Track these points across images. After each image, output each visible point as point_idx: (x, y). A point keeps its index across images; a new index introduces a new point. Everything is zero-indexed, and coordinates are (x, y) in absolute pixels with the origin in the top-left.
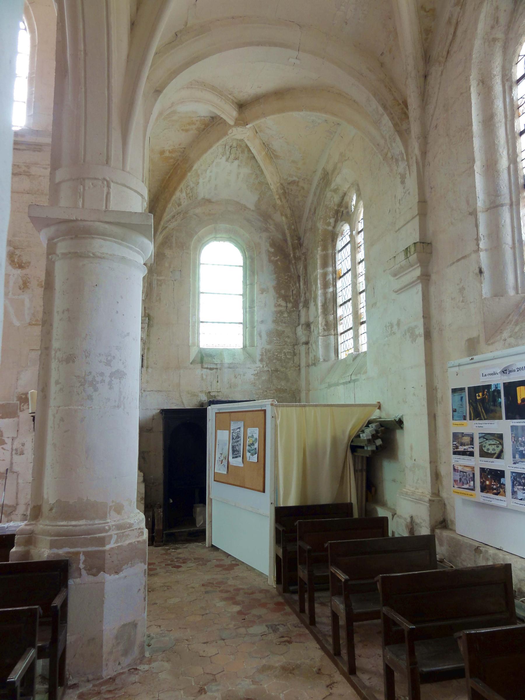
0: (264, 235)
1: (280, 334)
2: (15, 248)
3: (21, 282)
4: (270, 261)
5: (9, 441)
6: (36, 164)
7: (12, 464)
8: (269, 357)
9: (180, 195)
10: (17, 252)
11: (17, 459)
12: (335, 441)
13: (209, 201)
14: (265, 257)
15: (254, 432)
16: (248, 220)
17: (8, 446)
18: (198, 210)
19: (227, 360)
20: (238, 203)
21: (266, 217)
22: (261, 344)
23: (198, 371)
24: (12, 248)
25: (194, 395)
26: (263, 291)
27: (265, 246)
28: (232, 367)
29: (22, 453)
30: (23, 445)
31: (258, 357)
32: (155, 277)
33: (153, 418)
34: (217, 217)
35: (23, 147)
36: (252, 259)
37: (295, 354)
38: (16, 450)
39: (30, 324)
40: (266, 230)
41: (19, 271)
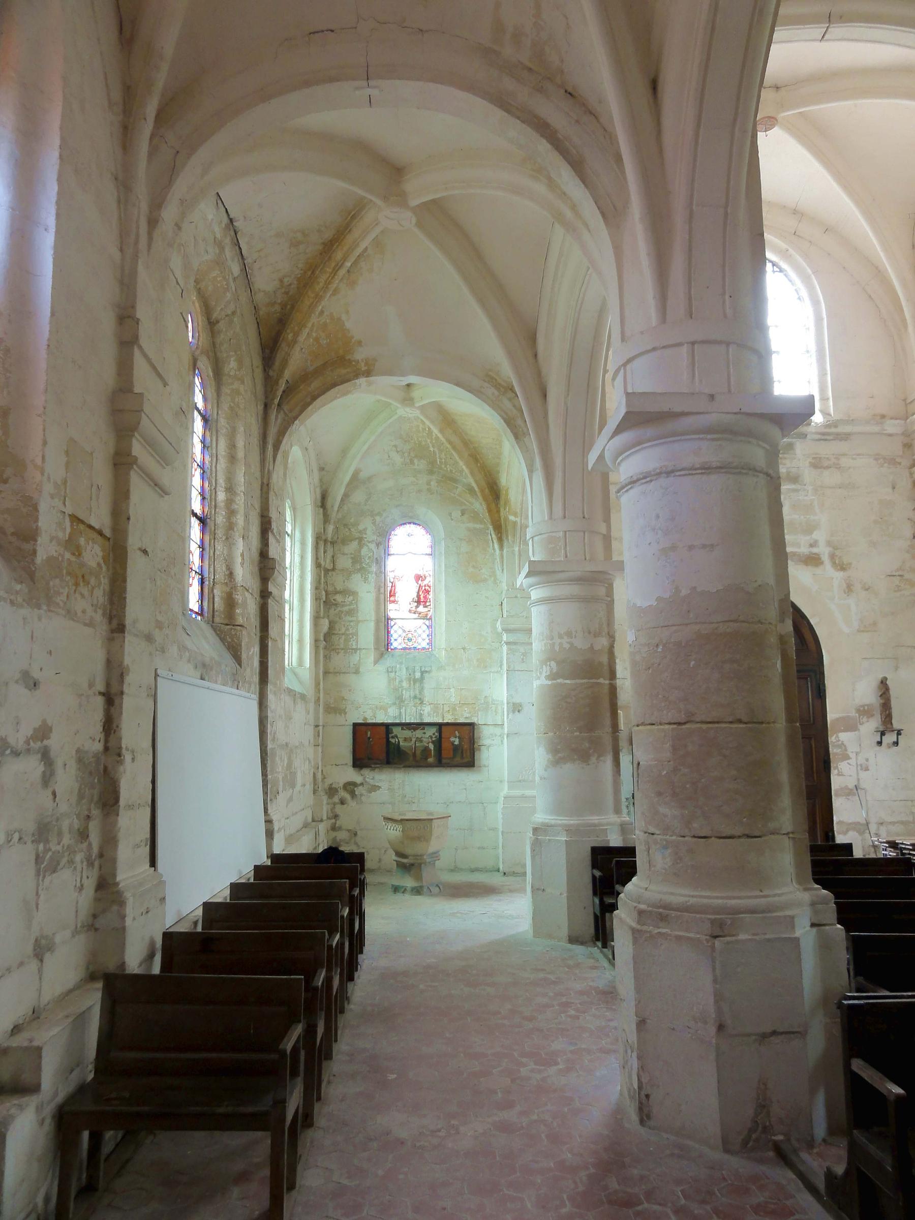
2: (835, 548)
3: (845, 586)
5: (852, 756)
6: (844, 455)
7: (858, 780)
10: (837, 553)
11: (863, 775)
17: (853, 762)
24: (831, 549)
29: (867, 769)
30: (867, 760)
35: (831, 437)
38: (861, 765)
39: (858, 631)
41: (842, 573)
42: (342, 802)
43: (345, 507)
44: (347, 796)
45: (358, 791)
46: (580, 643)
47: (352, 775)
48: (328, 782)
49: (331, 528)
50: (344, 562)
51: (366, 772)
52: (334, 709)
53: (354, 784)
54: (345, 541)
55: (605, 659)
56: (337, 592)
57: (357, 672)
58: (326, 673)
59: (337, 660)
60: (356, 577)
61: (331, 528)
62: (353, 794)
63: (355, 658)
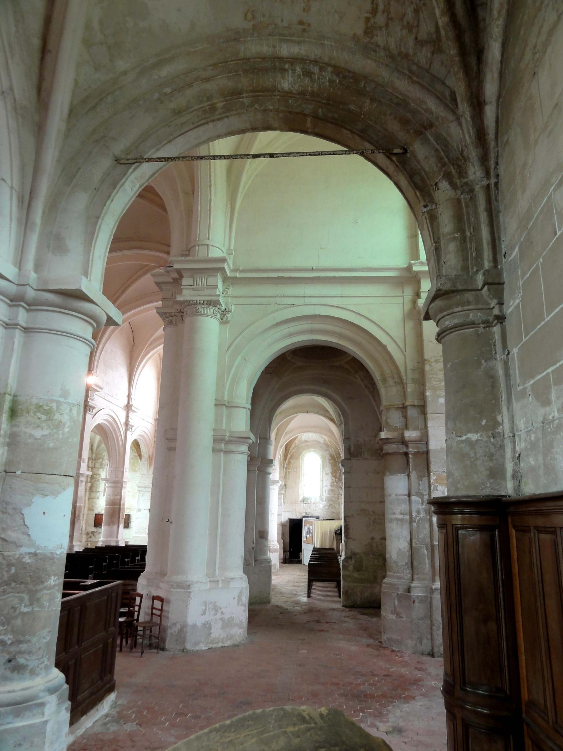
0: (327, 452)
1: (332, 491)
4: (330, 463)
8: (328, 500)
9: (296, 441)
12: (331, 531)
13: (307, 441)
14: (327, 461)
15: (311, 527)
16: (321, 447)
18: (303, 445)
19: (313, 501)
20: (317, 441)
21: (327, 446)
22: (326, 494)
23: (303, 505)
25: (301, 513)
26: (326, 474)
27: (328, 457)
28: (314, 503)
31: (324, 500)
32: (288, 470)
33: (287, 521)
34: (309, 445)
36: (323, 462)
37: (338, 498)
40: (328, 450)
42: (90, 537)
43: (99, 449)
44: (92, 535)
45: (95, 534)
46: (112, 498)
47: (94, 529)
48: (87, 530)
49: (94, 456)
50: (98, 465)
51: (98, 528)
52: (91, 509)
53: (94, 532)
54: (99, 459)
55: (118, 501)
56: (95, 474)
57: (98, 498)
58: (89, 499)
59: (93, 495)
60: (101, 470)
61: (94, 456)
62: (94, 535)
63: (98, 494)
